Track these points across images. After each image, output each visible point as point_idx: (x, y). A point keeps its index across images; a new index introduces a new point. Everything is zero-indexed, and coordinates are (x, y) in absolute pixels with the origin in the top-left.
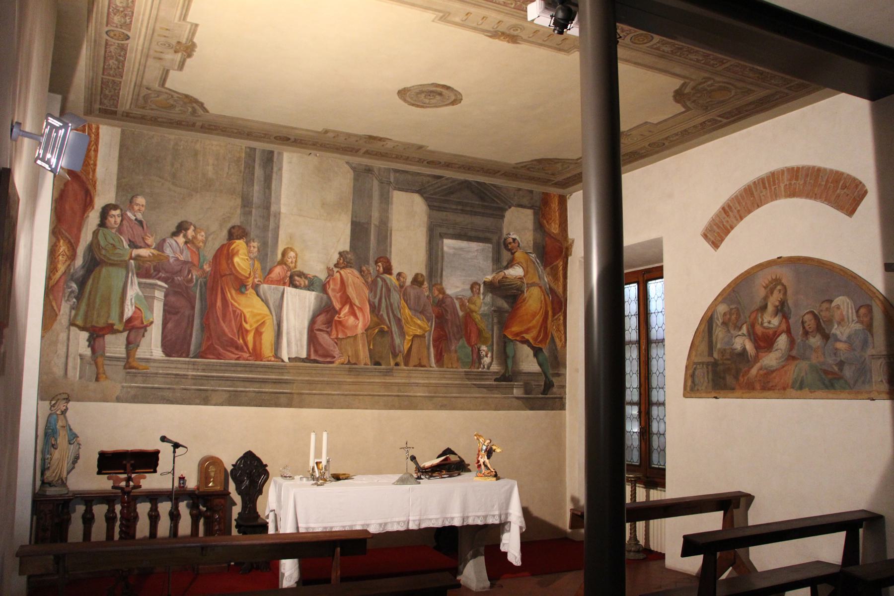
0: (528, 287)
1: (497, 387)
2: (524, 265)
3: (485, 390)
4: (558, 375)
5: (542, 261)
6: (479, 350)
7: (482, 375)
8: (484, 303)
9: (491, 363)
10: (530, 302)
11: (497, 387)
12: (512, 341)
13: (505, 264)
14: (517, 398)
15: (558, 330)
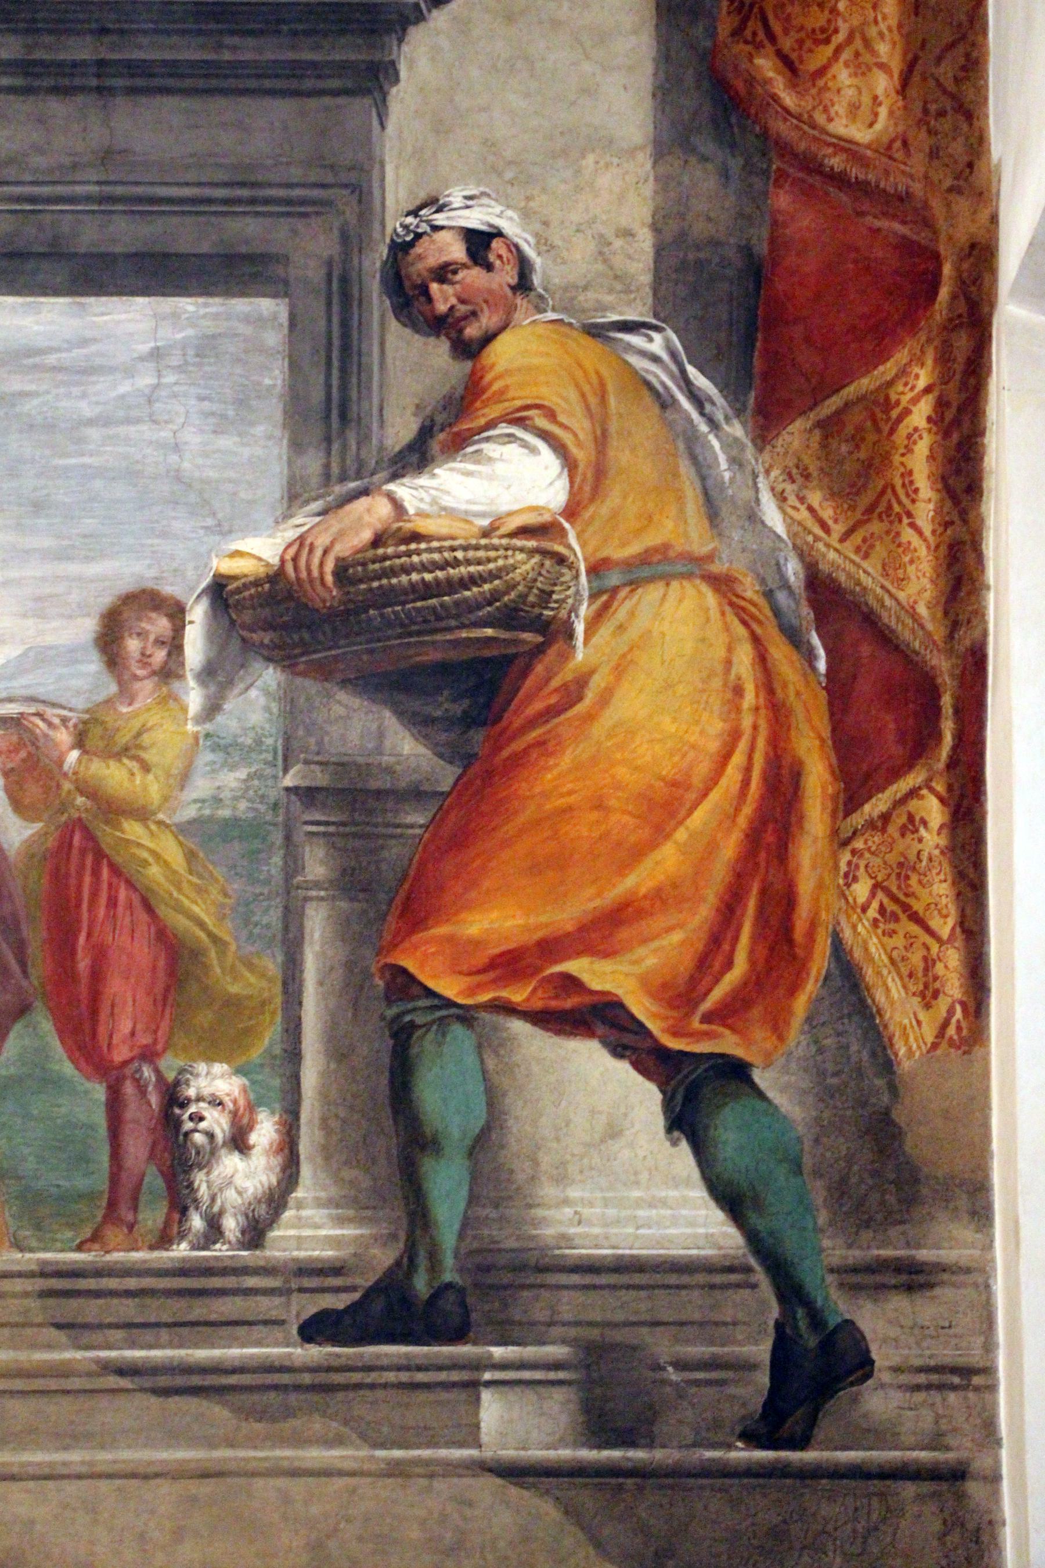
0: (606, 601)
1: (323, 1387)
2: (577, 425)
3: (218, 1412)
4: (914, 1278)
5: (734, 389)
6: (173, 1098)
7: (197, 1293)
8: (209, 748)
9: (277, 1200)
10: (631, 704)
11: (323, 1387)
12: (466, 1016)
13: (400, 429)
14: (514, 1473)
15: (899, 908)
